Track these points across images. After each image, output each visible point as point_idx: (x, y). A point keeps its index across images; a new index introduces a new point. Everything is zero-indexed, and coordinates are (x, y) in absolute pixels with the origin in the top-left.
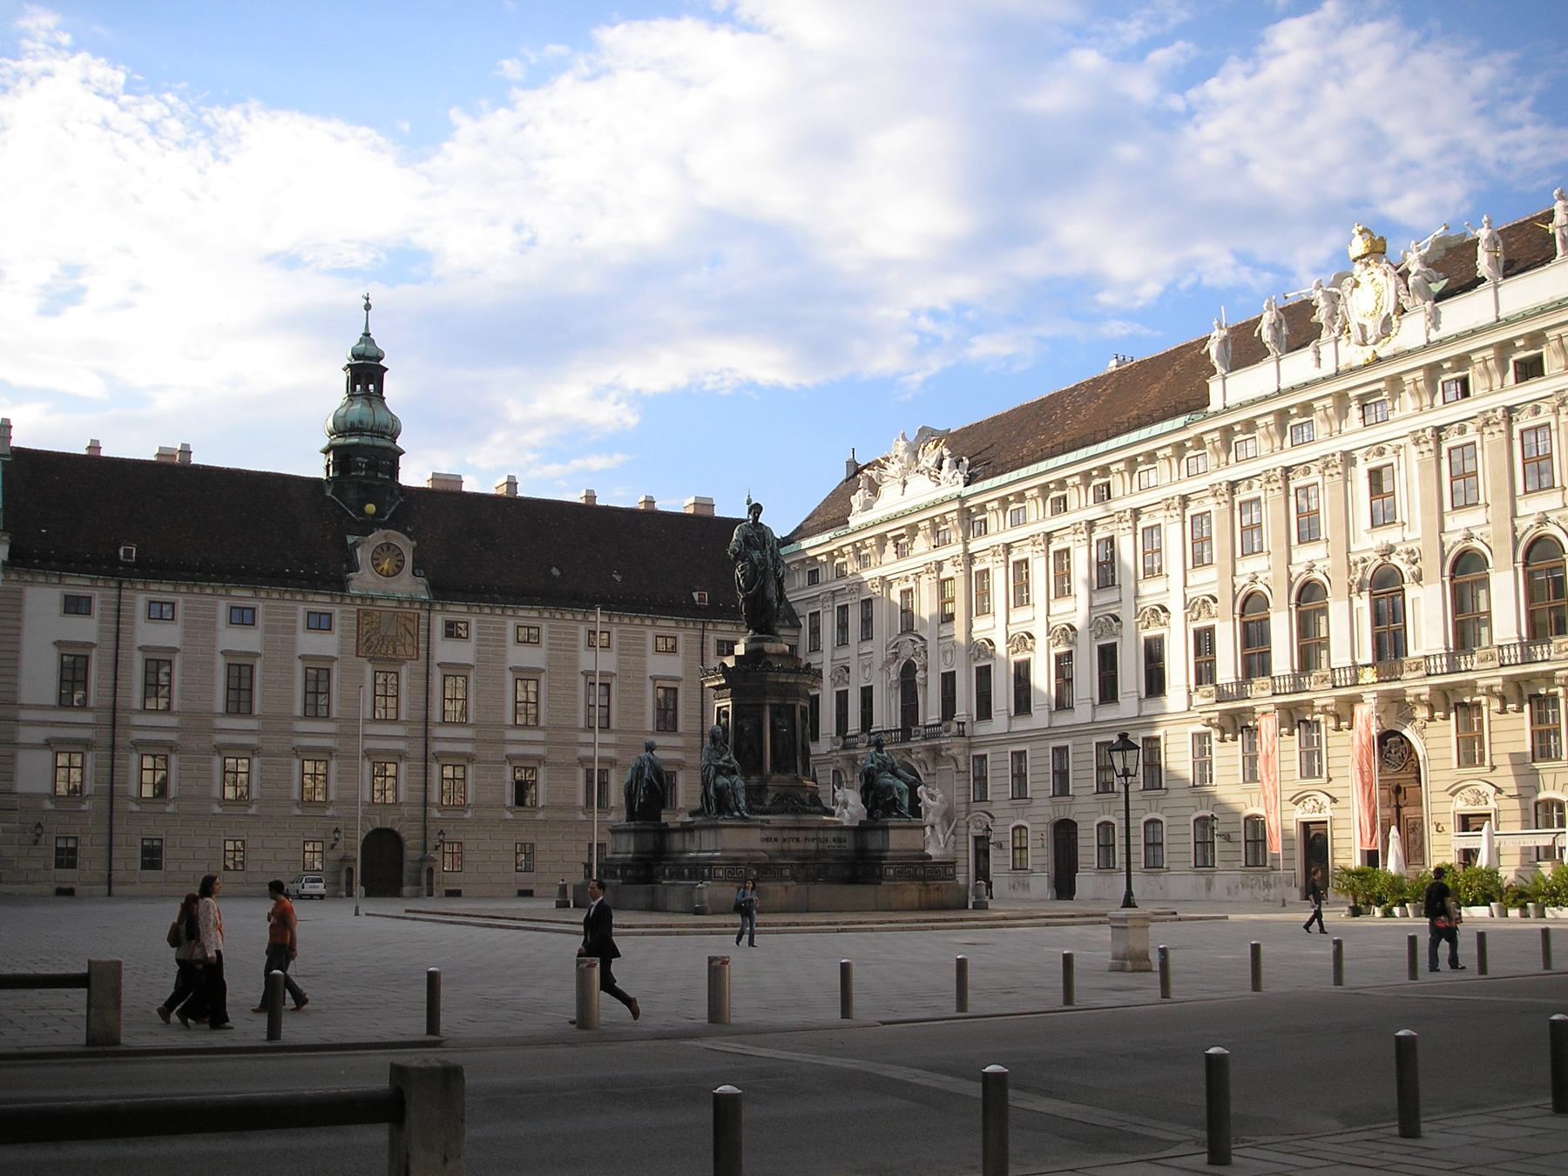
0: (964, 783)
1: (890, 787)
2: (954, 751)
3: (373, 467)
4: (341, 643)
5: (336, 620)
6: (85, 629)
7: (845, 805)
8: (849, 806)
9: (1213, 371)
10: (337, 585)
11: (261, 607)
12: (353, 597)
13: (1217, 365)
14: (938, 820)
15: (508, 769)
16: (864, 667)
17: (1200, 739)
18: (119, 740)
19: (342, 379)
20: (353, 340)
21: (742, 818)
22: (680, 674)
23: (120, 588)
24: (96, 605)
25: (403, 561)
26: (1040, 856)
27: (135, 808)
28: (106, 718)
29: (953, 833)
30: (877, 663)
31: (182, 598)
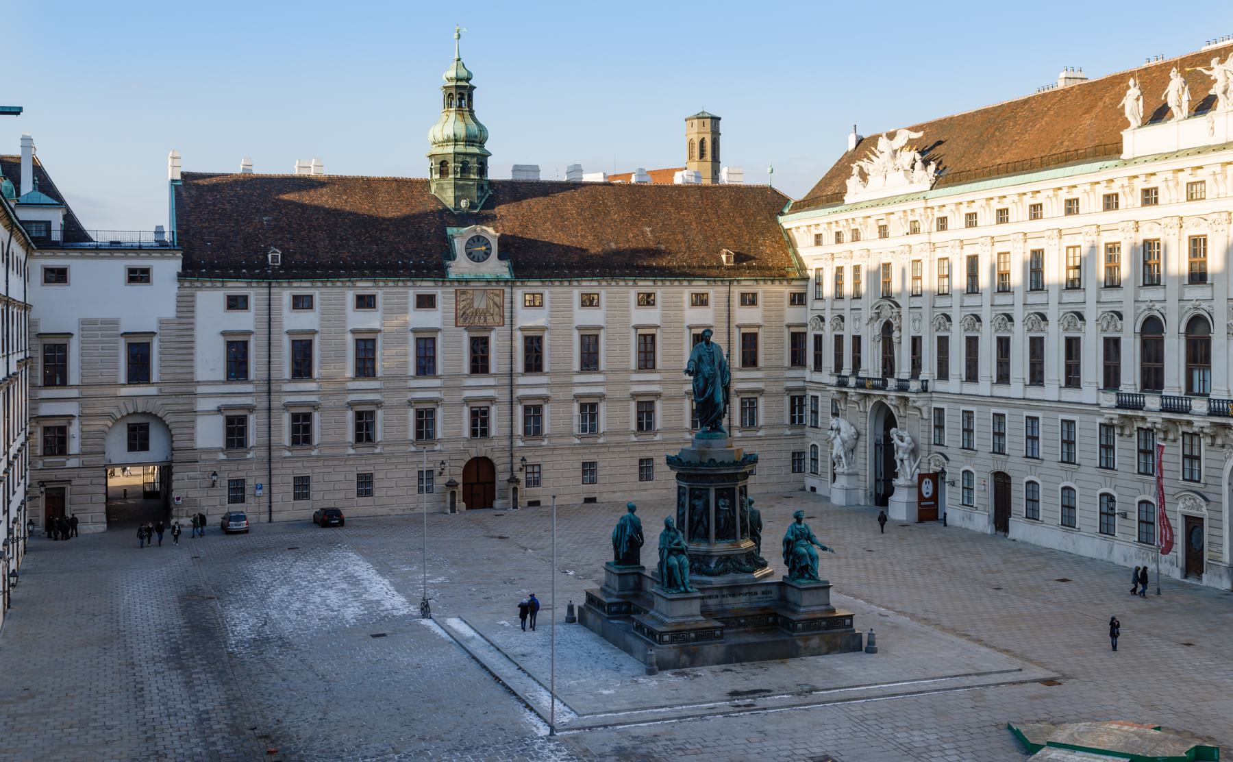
0: (926, 429)
1: (803, 555)
2: (918, 404)
4: (444, 318)
6: (242, 321)
7: (838, 430)
8: (776, 569)
9: (1127, 124)
10: (438, 271)
11: (380, 294)
12: (452, 281)
13: (1130, 119)
14: (906, 456)
16: (855, 320)
17: (1107, 428)
18: (274, 404)
21: (687, 592)
23: (270, 287)
24: (252, 302)
25: (489, 249)
26: (984, 495)
27: (288, 454)
29: (918, 467)
30: (865, 320)
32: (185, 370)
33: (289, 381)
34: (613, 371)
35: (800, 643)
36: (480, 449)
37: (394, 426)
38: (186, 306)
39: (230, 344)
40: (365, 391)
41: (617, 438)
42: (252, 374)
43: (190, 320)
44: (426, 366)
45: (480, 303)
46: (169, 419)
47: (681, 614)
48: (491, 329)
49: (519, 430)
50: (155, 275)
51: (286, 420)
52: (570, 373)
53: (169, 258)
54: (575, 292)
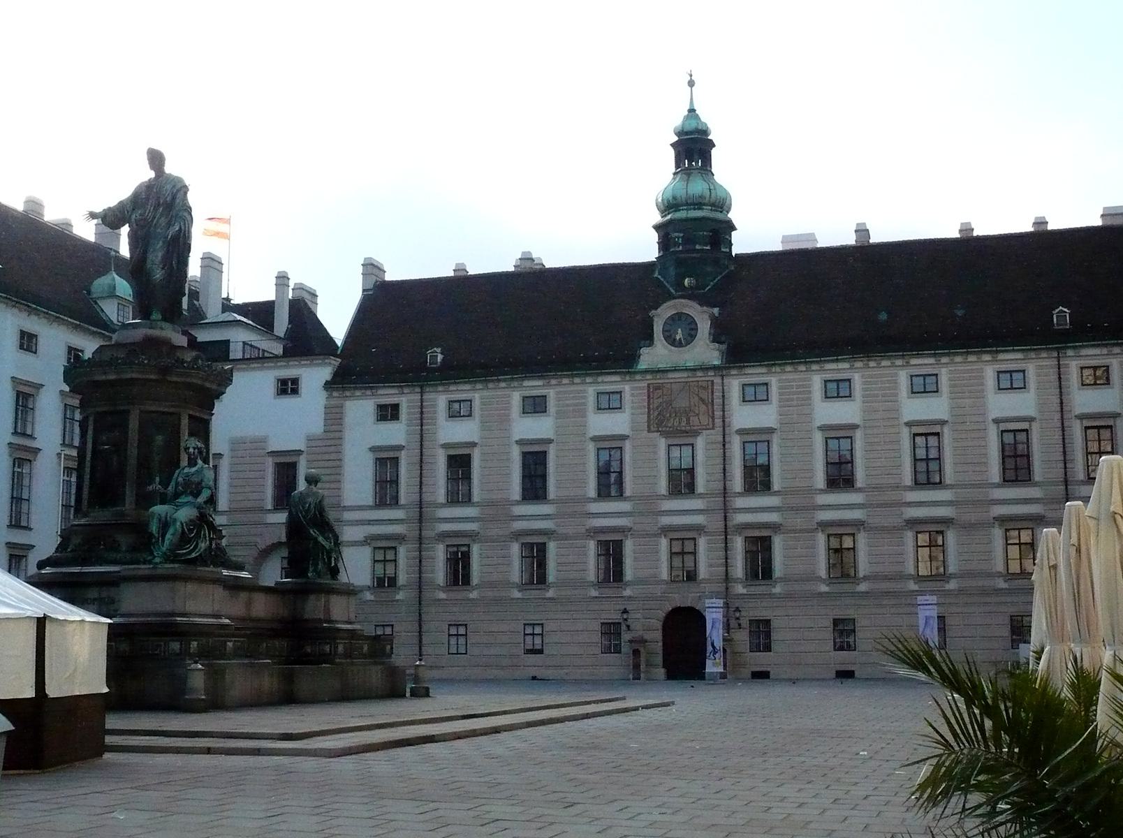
3: (688, 241)
4: (633, 421)
5: (627, 397)
11: (551, 393)
15: (821, 538)
19: (668, 158)
20: (677, 118)
22: (1031, 412)
23: (422, 393)
24: (404, 412)
27: (442, 595)
28: (414, 513)
31: (477, 395)
34: (878, 488)
36: (684, 597)
37: (574, 562)
38: (334, 418)
39: (381, 463)
40: (534, 516)
41: (885, 586)
44: (610, 481)
45: (681, 403)
48: (696, 434)
49: (739, 569)
50: (304, 386)
51: (439, 554)
52: (812, 491)
53: (318, 365)
54: (815, 378)
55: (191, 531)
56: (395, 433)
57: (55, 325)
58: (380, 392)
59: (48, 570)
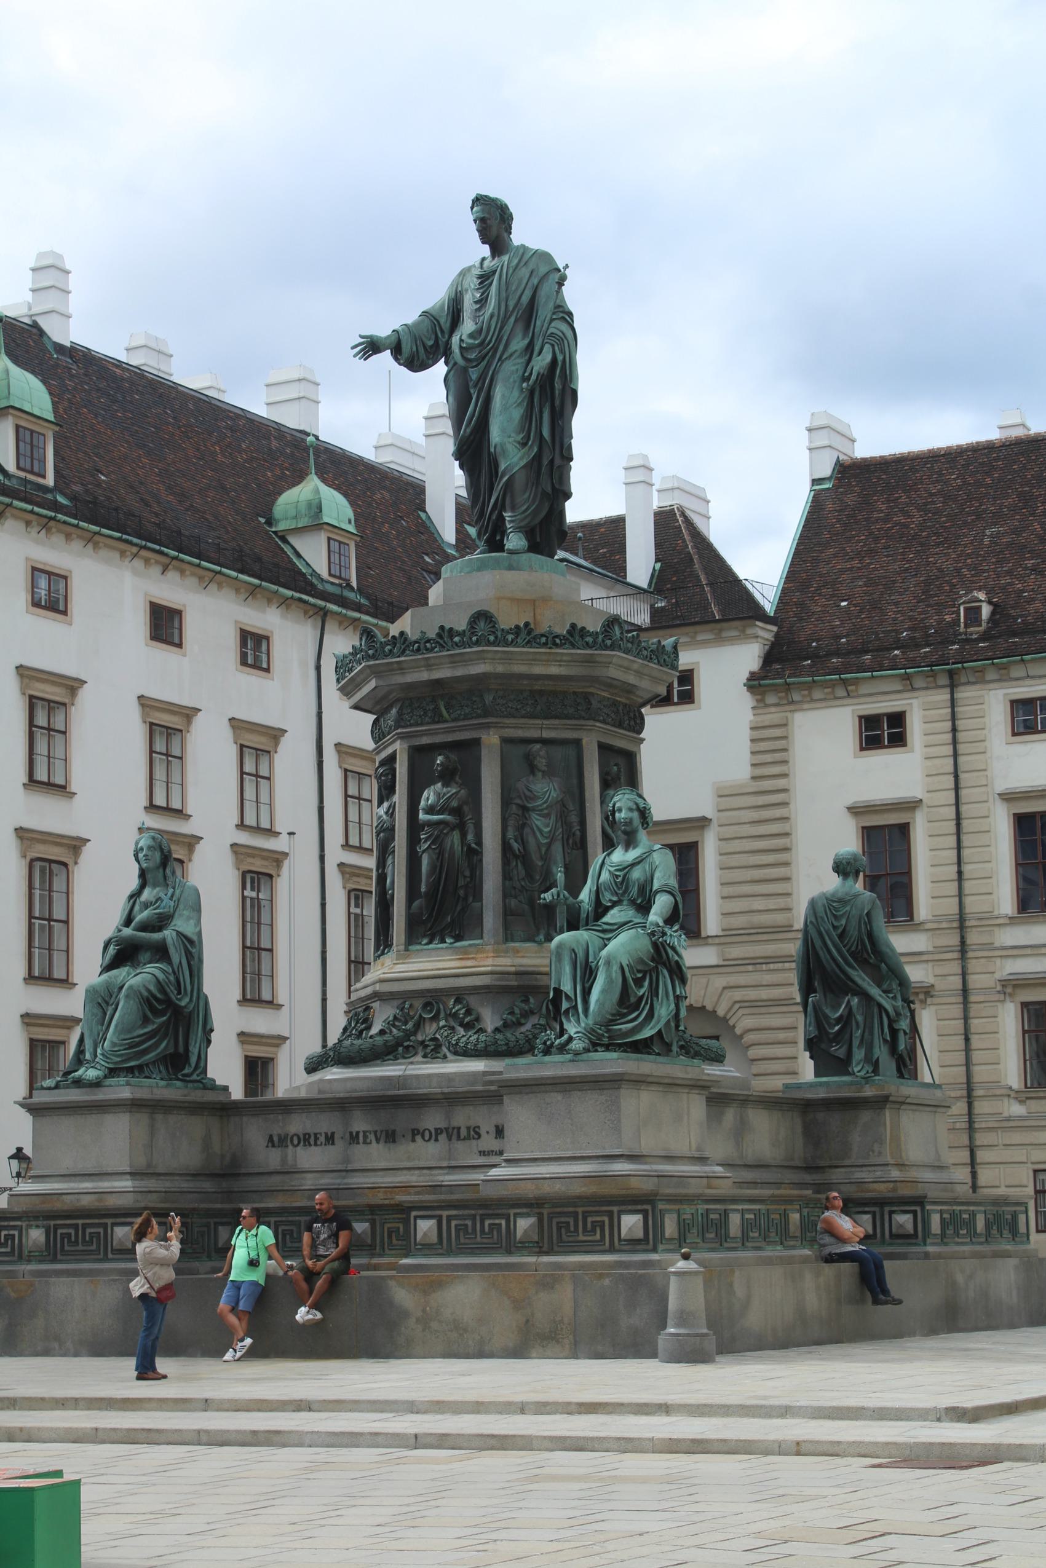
23: (953, 687)
24: (915, 727)
32: (772, 903)
33: (1012, 921)
35: (403, 1296)
38: (771, 752)
42: (923, 908)
43: (781, 783)
46: (743, 1022)
47: (67, 1164)
50: (704, 686)
53: (732, 640)
55: (639, 982)
56: (896, 776)
57: (213, 587)
58: (864, 689)
59: (333, 1073)
